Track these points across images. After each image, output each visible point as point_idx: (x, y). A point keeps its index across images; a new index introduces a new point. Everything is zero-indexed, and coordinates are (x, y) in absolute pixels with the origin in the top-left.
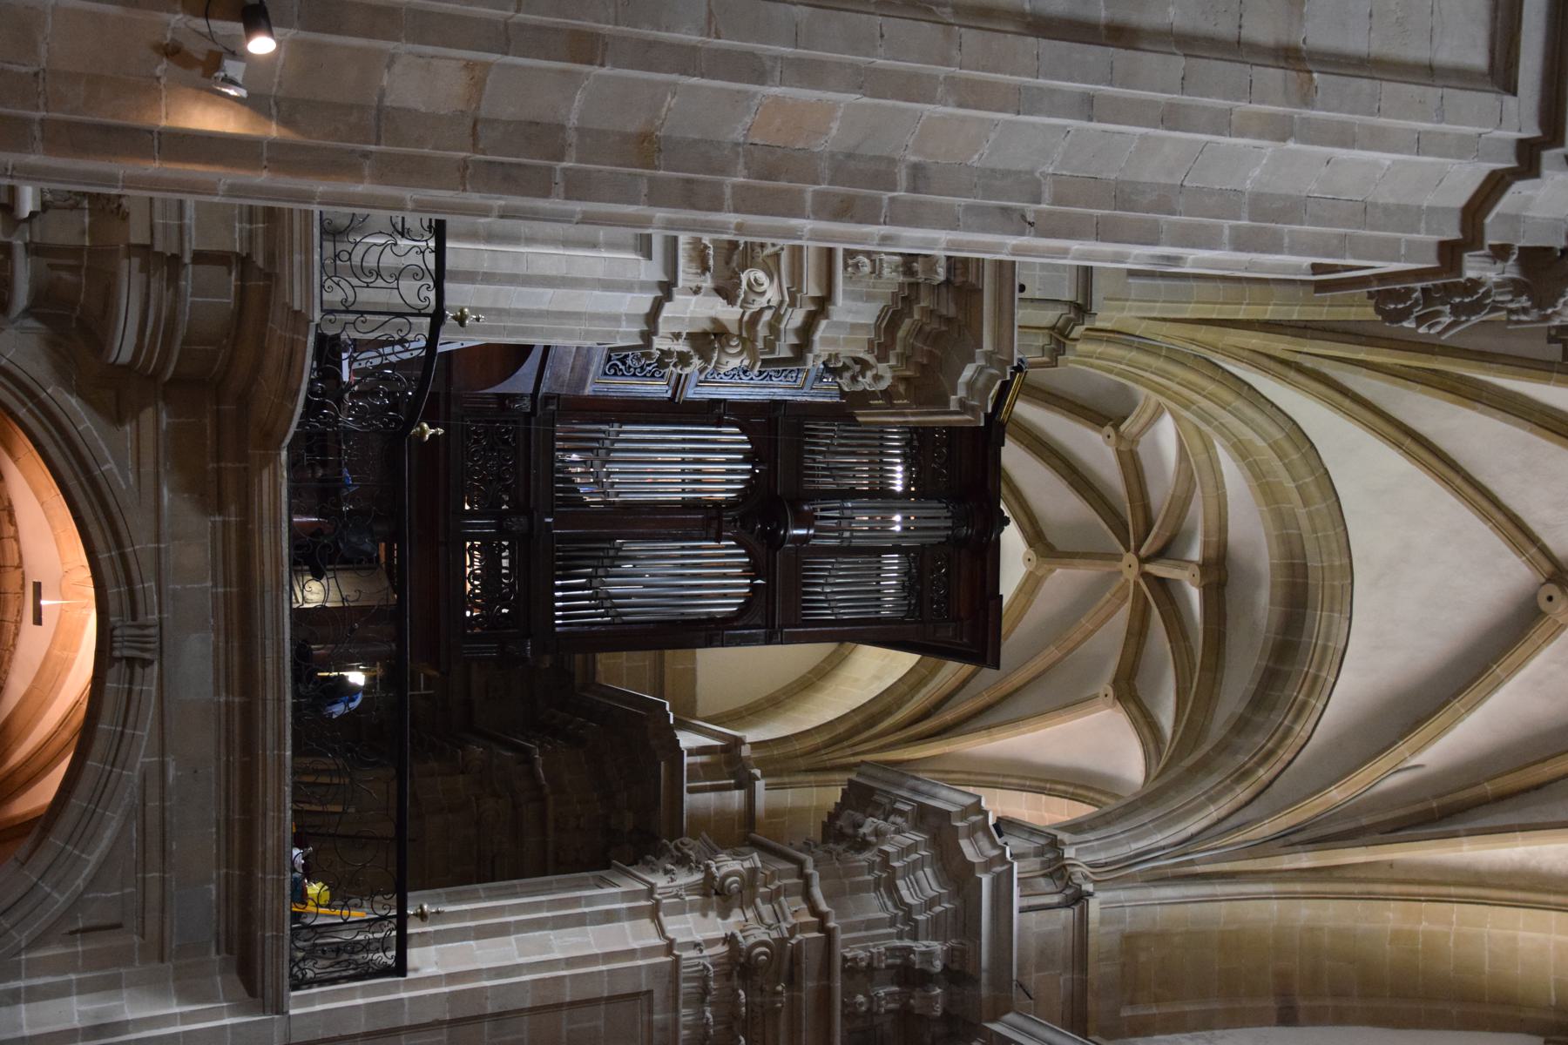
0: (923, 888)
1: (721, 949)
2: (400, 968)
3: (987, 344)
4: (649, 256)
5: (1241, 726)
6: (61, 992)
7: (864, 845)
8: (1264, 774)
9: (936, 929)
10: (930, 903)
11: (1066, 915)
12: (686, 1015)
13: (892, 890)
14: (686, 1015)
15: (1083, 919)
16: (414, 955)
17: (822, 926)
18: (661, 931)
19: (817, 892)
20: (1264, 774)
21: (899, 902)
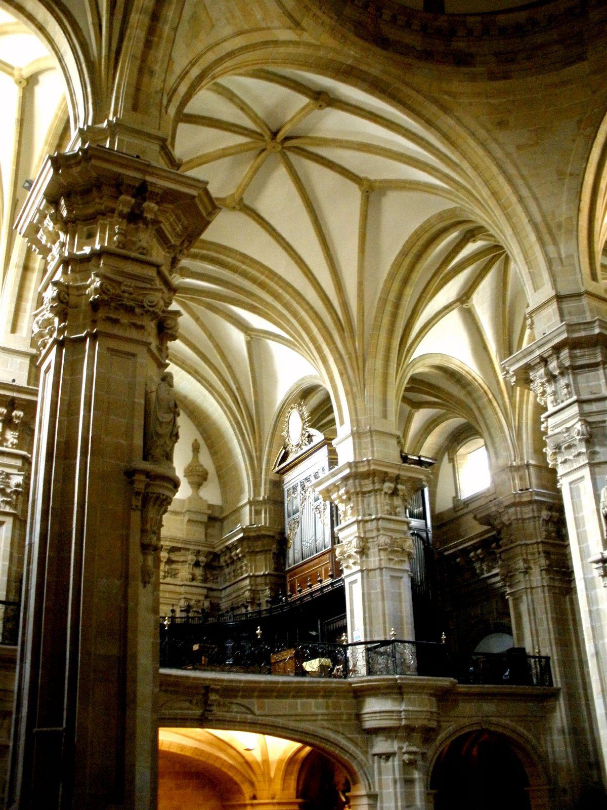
0: (528, 512)
1: (544, 572)
2: (548, 659)
3: (422, 477)
4: (401, 578)
5: (469, 394)
6: (552, 740)
7: (510, 524)
8: (491, 396)
9: (539, 511)
10: (533, 511)
11: (531, 469)
12: (557, 584)
13: (525, 519)
14: (557, 584)
15: (533, 465)
16: (543, 654)
17: (538, 543)
18: (537, 587)
19: (529, 542)
20: (491, 396)
21: (529, 519)
